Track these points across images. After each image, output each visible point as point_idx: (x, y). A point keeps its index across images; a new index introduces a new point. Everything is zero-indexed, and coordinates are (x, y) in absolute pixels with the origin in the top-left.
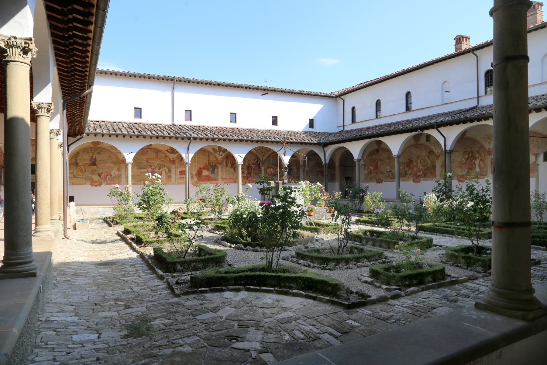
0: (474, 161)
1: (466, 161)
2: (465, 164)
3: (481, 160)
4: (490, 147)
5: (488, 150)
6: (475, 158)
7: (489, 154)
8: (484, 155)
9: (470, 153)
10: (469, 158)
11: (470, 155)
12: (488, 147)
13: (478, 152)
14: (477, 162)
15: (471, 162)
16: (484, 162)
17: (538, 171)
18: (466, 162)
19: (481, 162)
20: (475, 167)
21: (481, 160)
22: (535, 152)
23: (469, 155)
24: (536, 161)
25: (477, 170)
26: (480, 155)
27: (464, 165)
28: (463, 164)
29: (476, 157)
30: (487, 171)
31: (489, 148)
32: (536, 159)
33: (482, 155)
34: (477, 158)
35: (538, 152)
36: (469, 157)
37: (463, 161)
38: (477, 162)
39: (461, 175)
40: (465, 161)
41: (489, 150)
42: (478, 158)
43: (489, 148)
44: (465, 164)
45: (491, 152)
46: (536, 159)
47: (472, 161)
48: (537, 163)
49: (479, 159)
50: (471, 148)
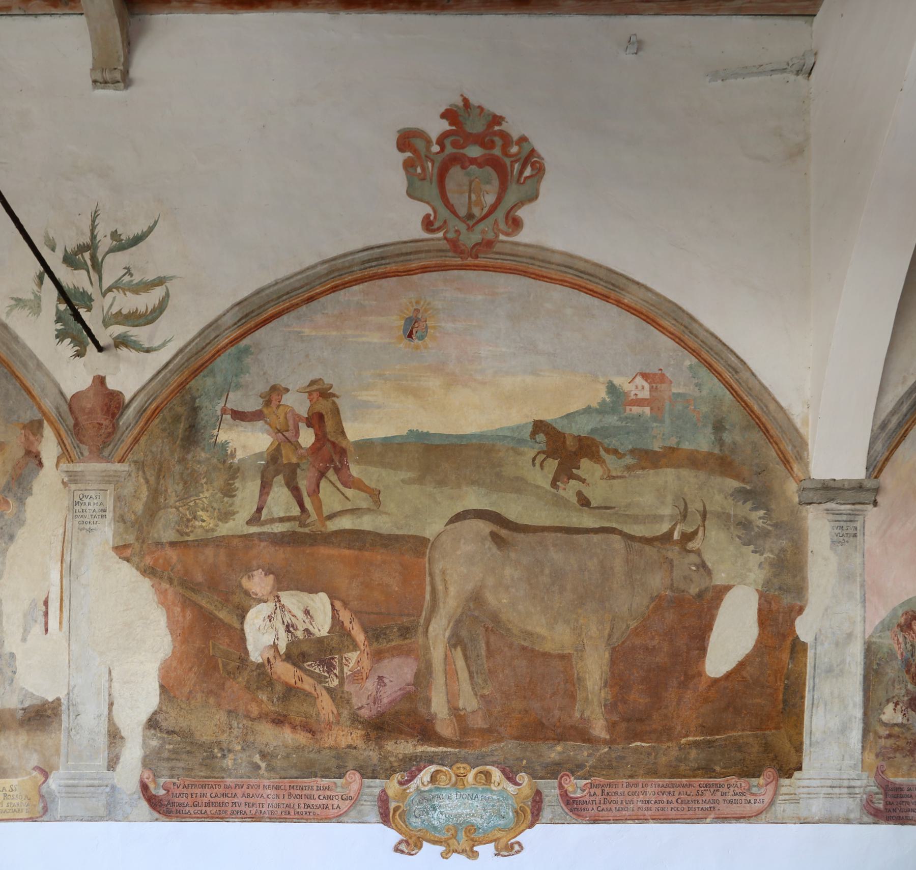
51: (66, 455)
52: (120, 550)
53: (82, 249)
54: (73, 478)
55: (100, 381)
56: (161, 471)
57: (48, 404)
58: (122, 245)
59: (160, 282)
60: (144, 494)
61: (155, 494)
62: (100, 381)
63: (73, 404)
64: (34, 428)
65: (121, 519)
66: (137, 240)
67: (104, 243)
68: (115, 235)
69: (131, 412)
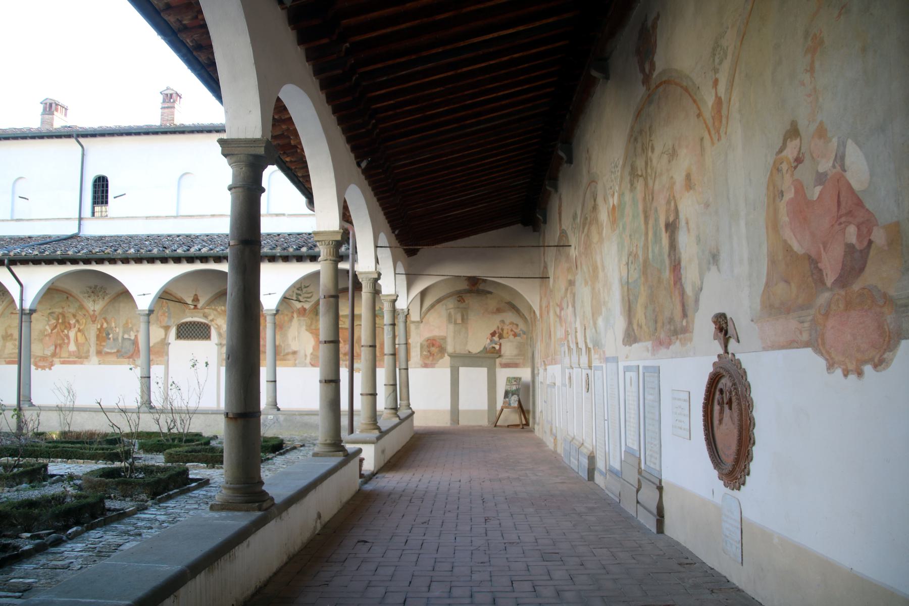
0: (66, 331)
1: (52, 330)
2: (49, 335)
3: (79, 330)
4: (95, 309)
5: (92, 313)
6: (69, 327)
7: (94, 322)
8: (84, 321)
9: (61, 316)
10: (58, 326)
11: (60, 321)
12: (92, 308)
13: (74, 316)
14: (72, 334)
15: (61, 333)
16: (83, 334)
17: (167, 354)
18: (51, 333)
19: (79, 334)
20: (68, 343)
21: (79, 330)
22: (164, 324)
23: (59, 319)
24: (165, 339)
25: (72, 347)
26: (78, 321)
27: (47, 338)
28: (46, 335)
29: (69, 324)
30: (88, 351)
31: (94, 311)
32: (166, 335)
33: (81, 322)
34: (72, 326)
35: (169, 324)
36: (58, 322)
37: (46, 330)
38: (72, 334)
39: (41, 357)
40: (50, 331)
41: (94, 315)
42: (75, 327)
43: (94, 311)
44: (49, 335)
45: (96, 317)
46: (166, 335)
47: (63, 331)
48: (166, 342)
49: (76, 329)
50: (63, 308)
51: (298, 317)
52: (306, 330)
53: (300, 288)
54: (299, 320)
55: (303, 306)
56: (312, 319)
57: (295, 309)
58: (306, 287)
59: (311, 293)
60: (310, 322)
61: (311, 322)
62: (303, 306)
63: (299, 309)
64: (293, 312)
65: (306, 326)
66: (308, 287)
67: (303, 287)
68: (304, 286)
69: (308, 311)
